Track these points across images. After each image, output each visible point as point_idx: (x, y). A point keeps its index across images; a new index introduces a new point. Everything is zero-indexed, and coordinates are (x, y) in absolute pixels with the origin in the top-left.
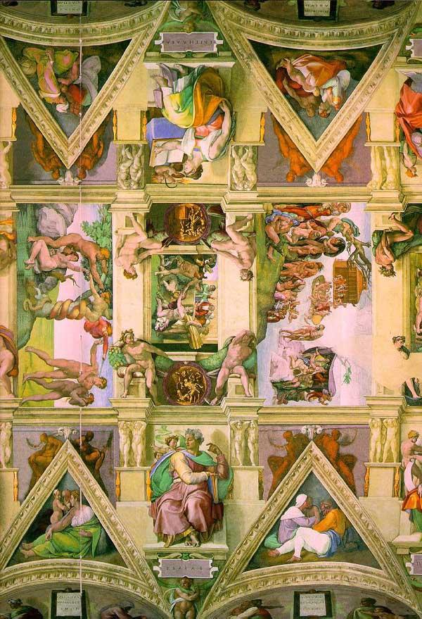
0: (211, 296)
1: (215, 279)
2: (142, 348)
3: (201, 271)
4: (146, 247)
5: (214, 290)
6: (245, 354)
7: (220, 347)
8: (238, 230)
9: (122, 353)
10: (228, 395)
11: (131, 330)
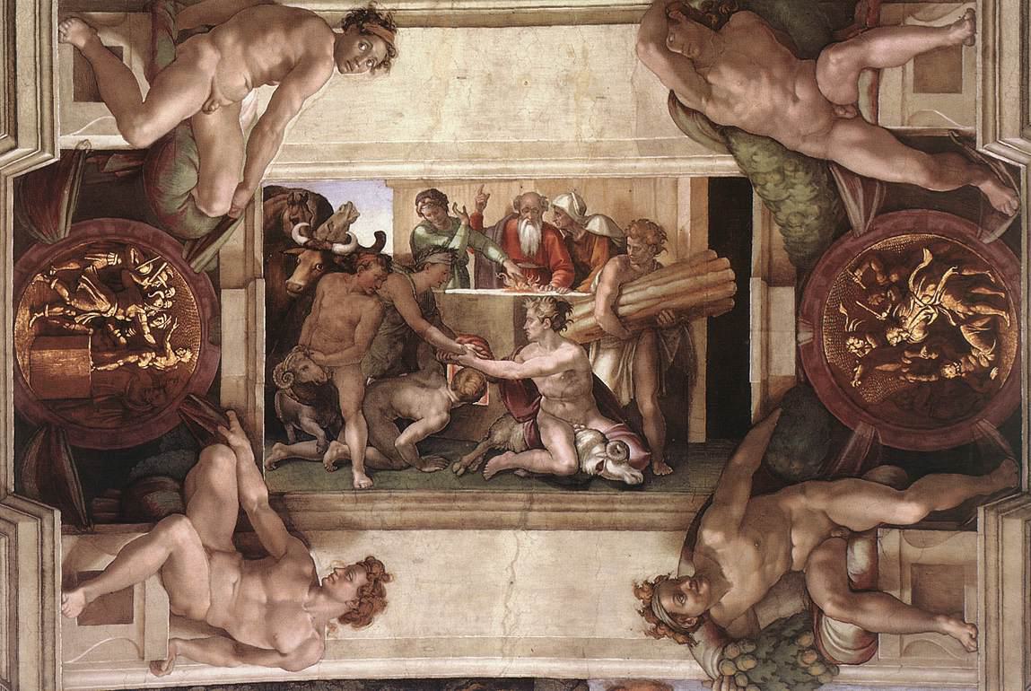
0: (471, 210)
1: (389, 193)
2: (728, 538)
3: (351, 263)
4: (230, 520)
5: (435, 198)
6: (760, 45)
7: (725, 166)
8: (144, 86)
9: (751, 639)
10: (968, 129)
11: (637, 591)
